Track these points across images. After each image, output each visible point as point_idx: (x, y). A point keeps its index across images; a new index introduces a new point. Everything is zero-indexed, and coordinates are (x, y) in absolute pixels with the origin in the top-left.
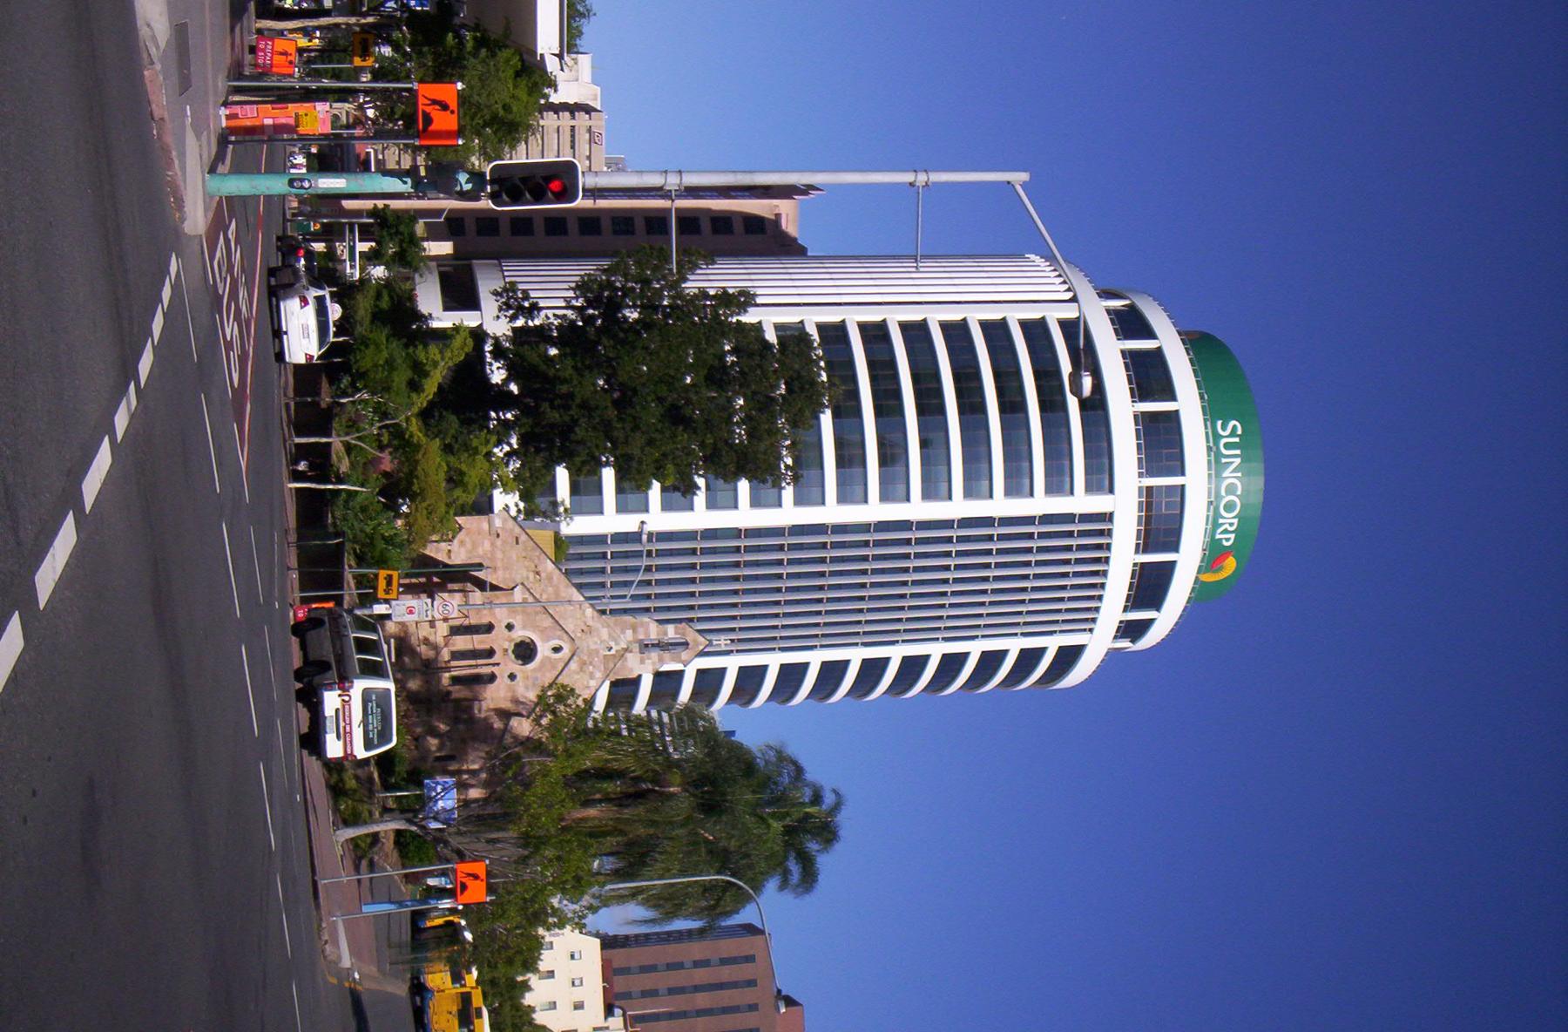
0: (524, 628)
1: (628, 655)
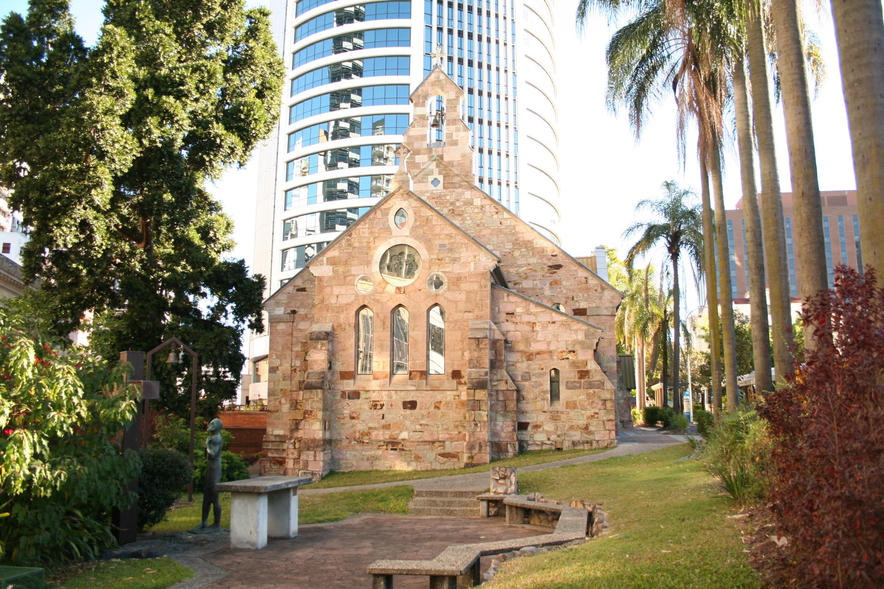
0: (368, 263)
1: (446, 159)
